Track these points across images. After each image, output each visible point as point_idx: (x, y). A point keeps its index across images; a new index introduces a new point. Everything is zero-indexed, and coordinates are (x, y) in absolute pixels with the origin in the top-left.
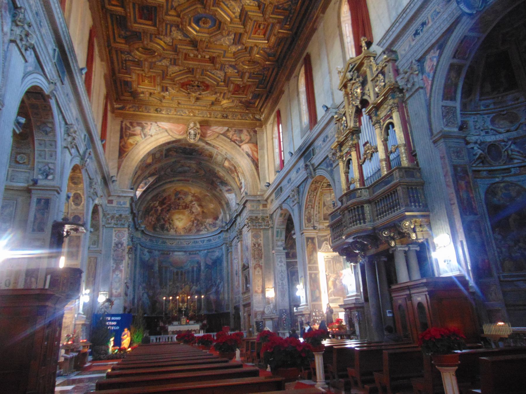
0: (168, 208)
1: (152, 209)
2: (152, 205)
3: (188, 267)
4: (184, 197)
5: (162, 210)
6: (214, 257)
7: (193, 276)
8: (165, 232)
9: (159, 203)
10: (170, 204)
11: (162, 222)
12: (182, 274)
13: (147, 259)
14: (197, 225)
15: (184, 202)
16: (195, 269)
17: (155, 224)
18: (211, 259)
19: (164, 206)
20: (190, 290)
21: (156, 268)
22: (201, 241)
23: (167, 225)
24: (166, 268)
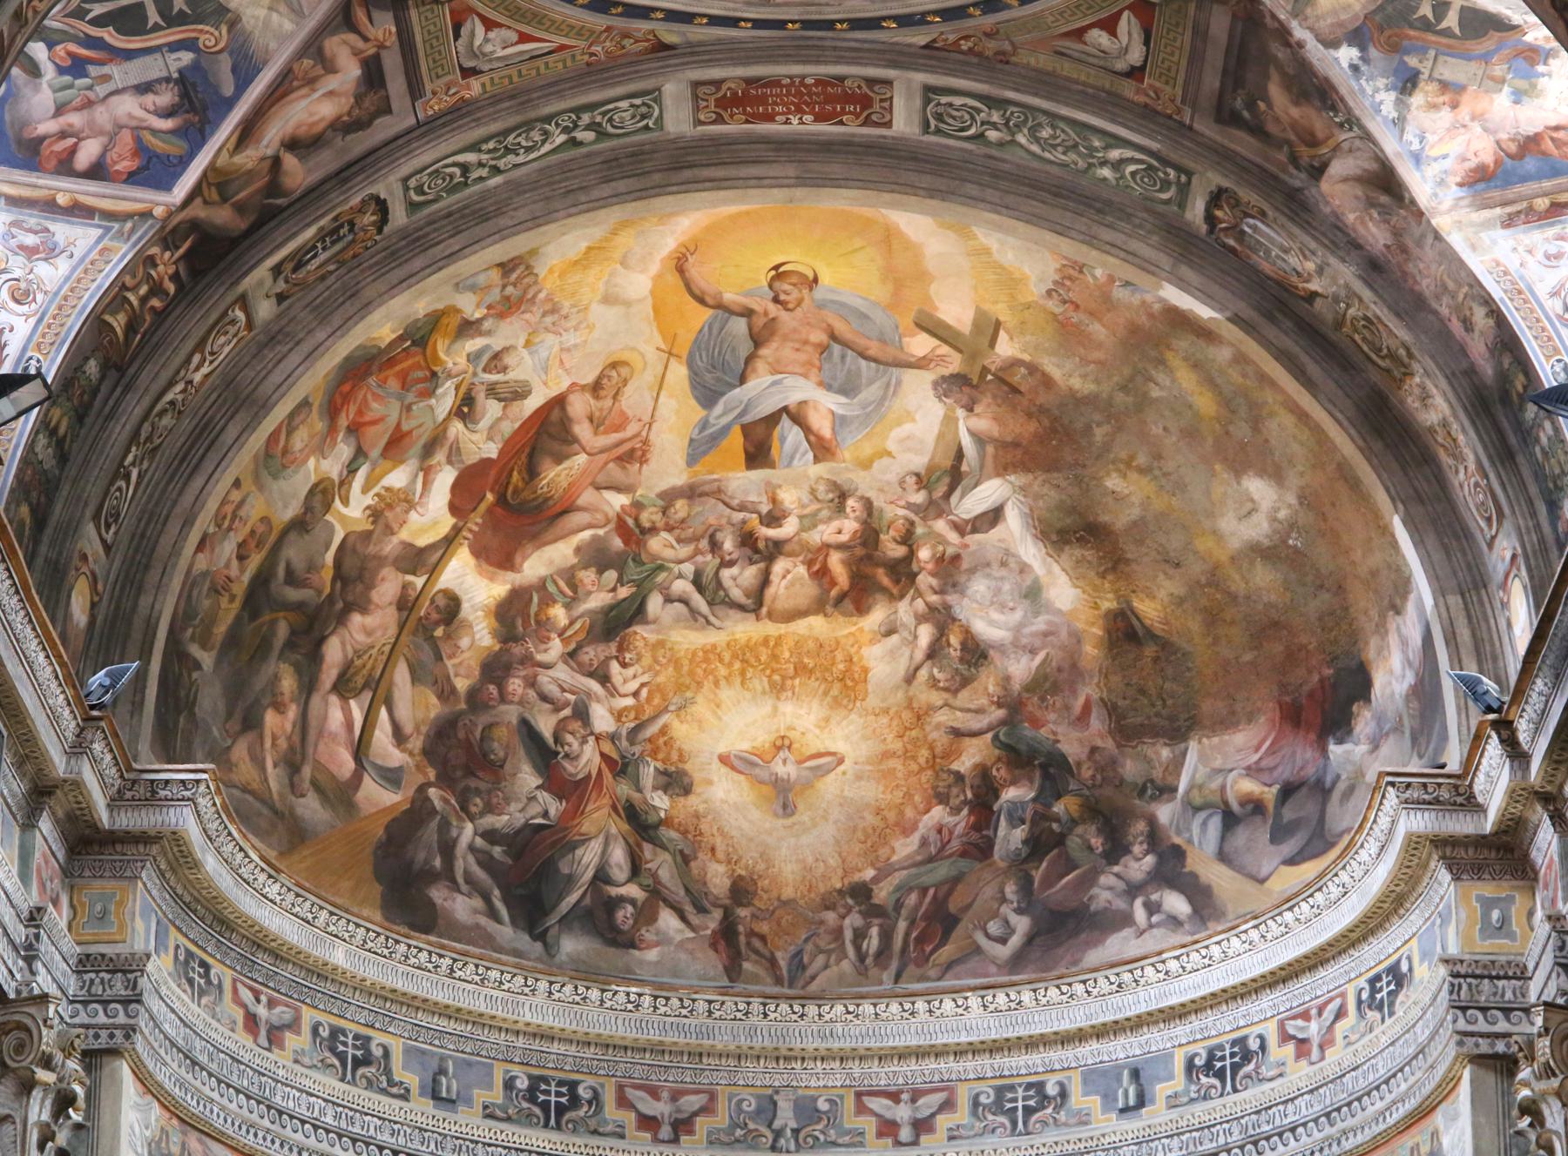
10: (632, 531)
14: (1045, 841)
17: (417, 814)
19: (538, 564)
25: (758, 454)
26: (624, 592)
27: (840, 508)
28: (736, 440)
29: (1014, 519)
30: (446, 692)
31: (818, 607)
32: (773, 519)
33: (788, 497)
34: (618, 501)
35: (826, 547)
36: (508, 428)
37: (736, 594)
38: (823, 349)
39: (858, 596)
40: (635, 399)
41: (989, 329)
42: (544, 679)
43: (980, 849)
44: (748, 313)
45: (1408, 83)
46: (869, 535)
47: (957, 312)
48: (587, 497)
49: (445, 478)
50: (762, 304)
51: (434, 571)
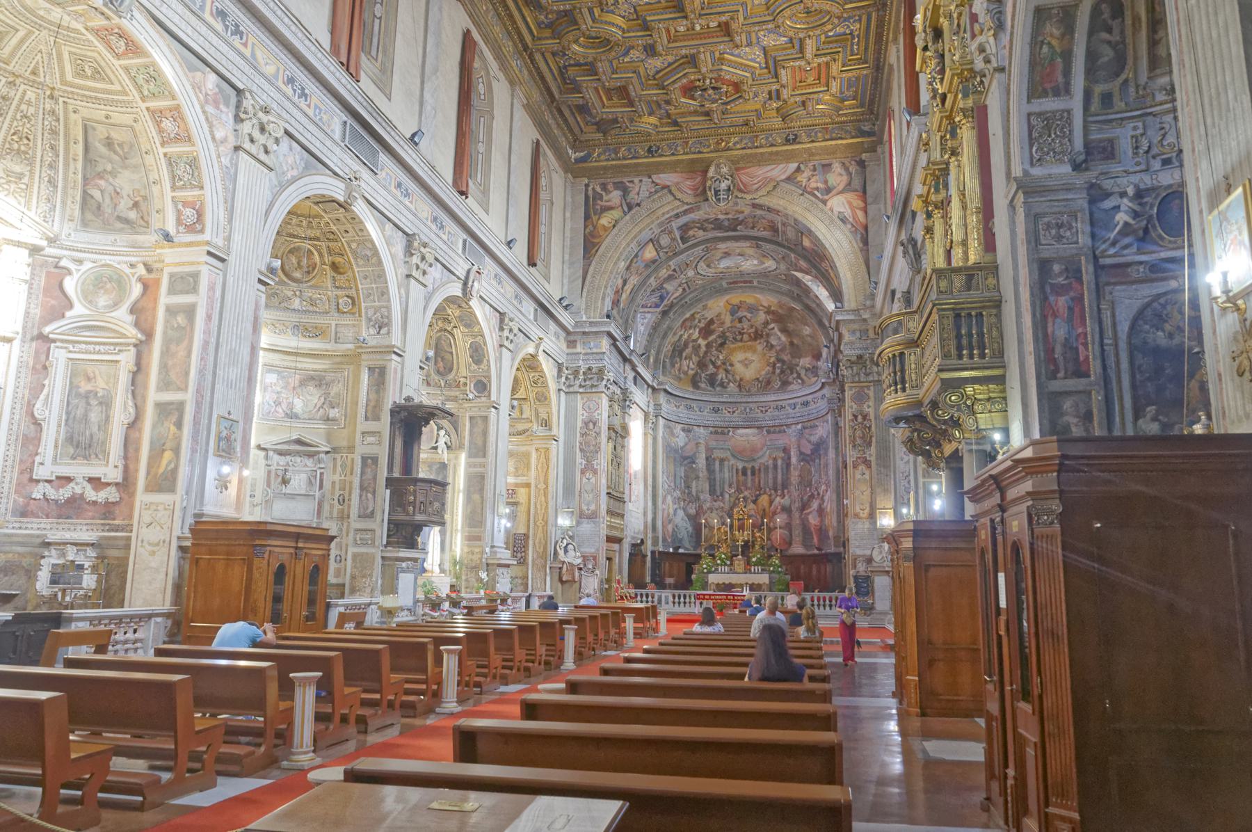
1: (686, 345)
2: (686, 336)
3: (765, 459)
4: (749, 315)
5: (708, 346)
6: (814, 439)
7: (775, 478)
8: (718, 389)
10: (723, 333)
11: (711, 369)
12: (753, 473)
13: (681, 444)
14: (782, 372)
15: (752, 326)
16: (779, 462)
17: (696, 374)
18: (810, 442)
19: (711, 338)
20: (771, 505)
21: (701, 462)
22: (790, 405)
23: (721, 375)
24: (722, 461)
39: (755, 339)
43: (774, 373)
46: (756, 331)
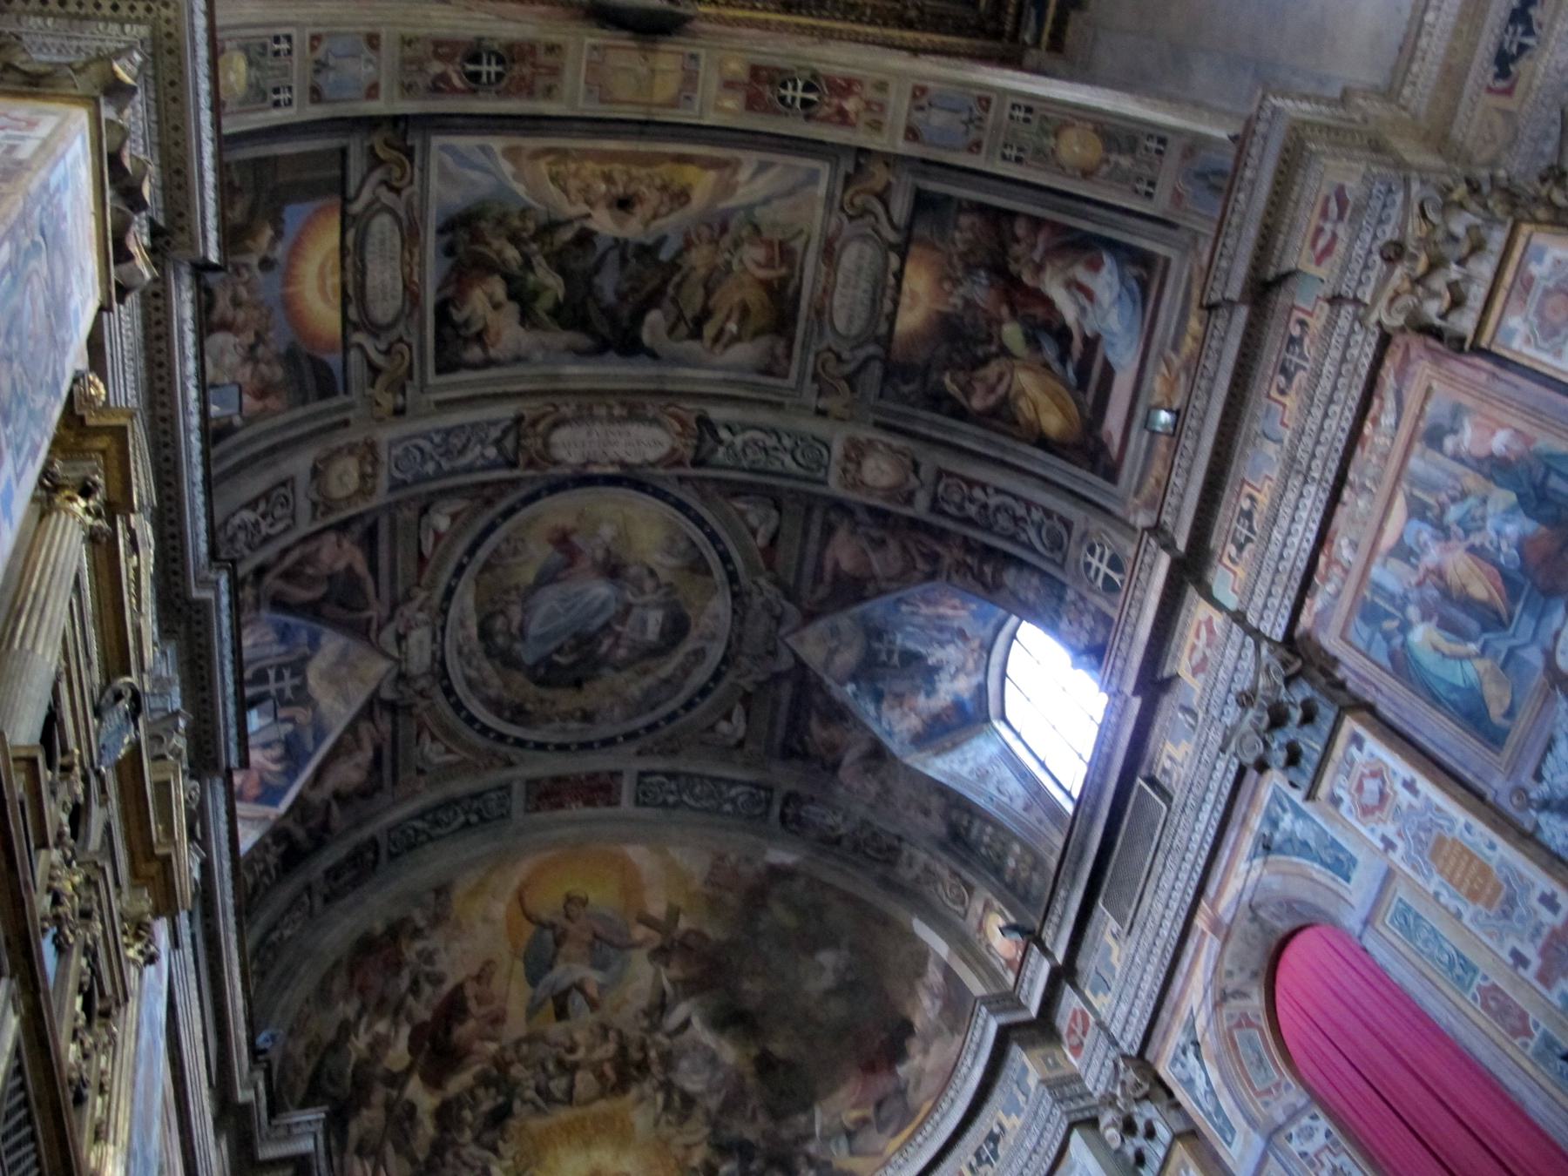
0: (488, 1101)
5: (446, 1115)
9: (414, 1046)
10: (501, 1064)
19: (458, 1083)
25: (561, 1013)
26: (501, 1100)
27: (605, 1038)
28: (550, 1005)
29: (696, 1022)
30: (413, 1161)
31: (602, 1095)
32: (572, 1050)
33: (579, 1036)
34: (492, 1047)
35: (601, 1062)
36: (436, 1002)
37: (559, 1095)
38: (591, 945)
39: (621, 1085)
40: (498, 984)
41: (674, 913)
42: (464, 1153)
44: (552, 926)
45: (878, 697)
46: (623, 1049)
47: (657, 909)
48: (477, 1045)
49: (405, 1031)
50: (560, 920)
51: (402, 1087)
